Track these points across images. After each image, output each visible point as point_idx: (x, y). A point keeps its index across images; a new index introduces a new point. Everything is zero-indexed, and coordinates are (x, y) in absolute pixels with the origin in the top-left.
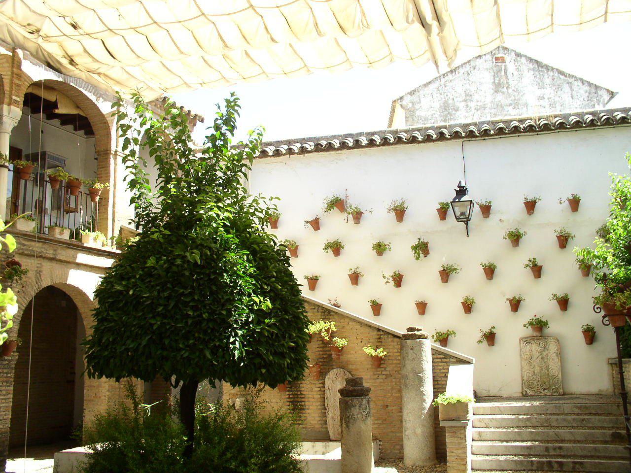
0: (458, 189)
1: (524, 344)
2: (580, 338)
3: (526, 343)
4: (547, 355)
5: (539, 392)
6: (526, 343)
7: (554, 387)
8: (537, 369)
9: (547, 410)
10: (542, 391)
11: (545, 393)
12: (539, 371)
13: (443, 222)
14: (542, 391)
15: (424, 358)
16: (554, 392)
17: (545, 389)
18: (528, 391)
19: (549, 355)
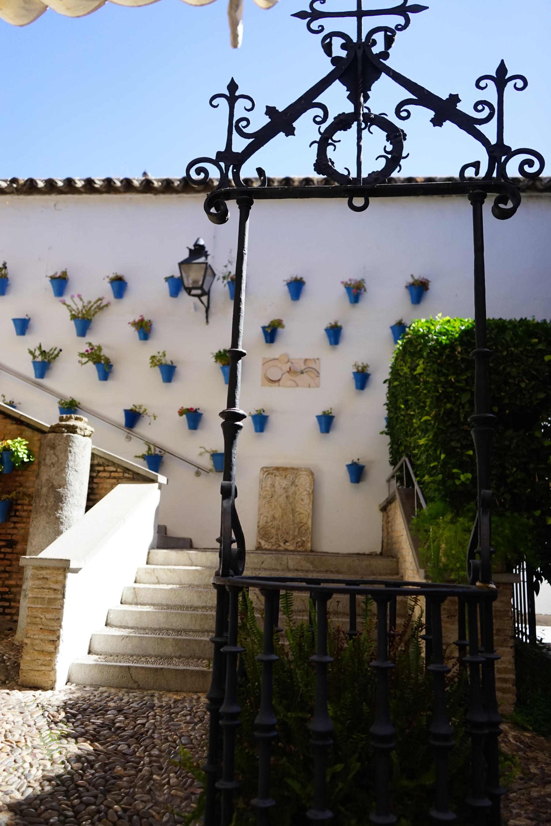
0: (193, 248)
1: (265, 476)
2: (344, 474)
3: (268, 474)
4: (295, 493)
5: (277, 546)
6: (268, 474)
7: (299, 540)
8: (278, 513)
9: (263, 563)
10: (282, 544)
11: (286, 547)
12: (280, 514)
13: (174, 299)
14: (282, 544)
15: (71, 464)
16: (299, 547)
17: (286, 542)
18: (263, 543)
19: (298, 493)
